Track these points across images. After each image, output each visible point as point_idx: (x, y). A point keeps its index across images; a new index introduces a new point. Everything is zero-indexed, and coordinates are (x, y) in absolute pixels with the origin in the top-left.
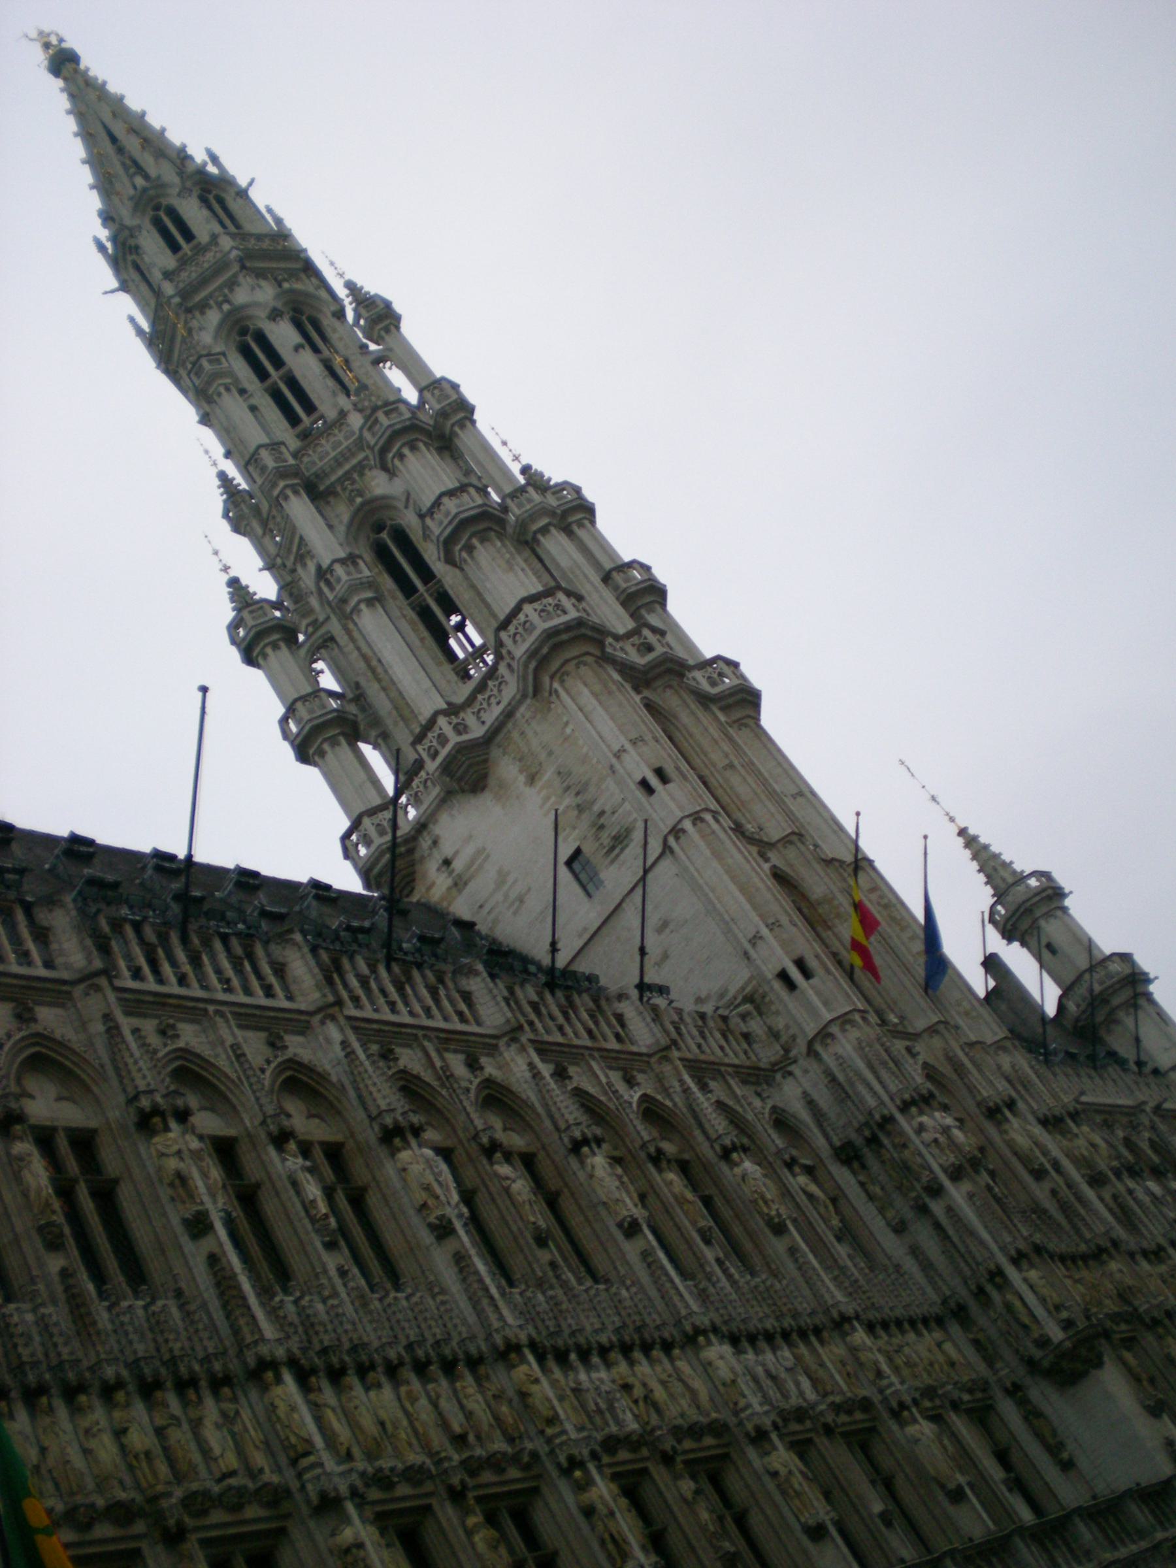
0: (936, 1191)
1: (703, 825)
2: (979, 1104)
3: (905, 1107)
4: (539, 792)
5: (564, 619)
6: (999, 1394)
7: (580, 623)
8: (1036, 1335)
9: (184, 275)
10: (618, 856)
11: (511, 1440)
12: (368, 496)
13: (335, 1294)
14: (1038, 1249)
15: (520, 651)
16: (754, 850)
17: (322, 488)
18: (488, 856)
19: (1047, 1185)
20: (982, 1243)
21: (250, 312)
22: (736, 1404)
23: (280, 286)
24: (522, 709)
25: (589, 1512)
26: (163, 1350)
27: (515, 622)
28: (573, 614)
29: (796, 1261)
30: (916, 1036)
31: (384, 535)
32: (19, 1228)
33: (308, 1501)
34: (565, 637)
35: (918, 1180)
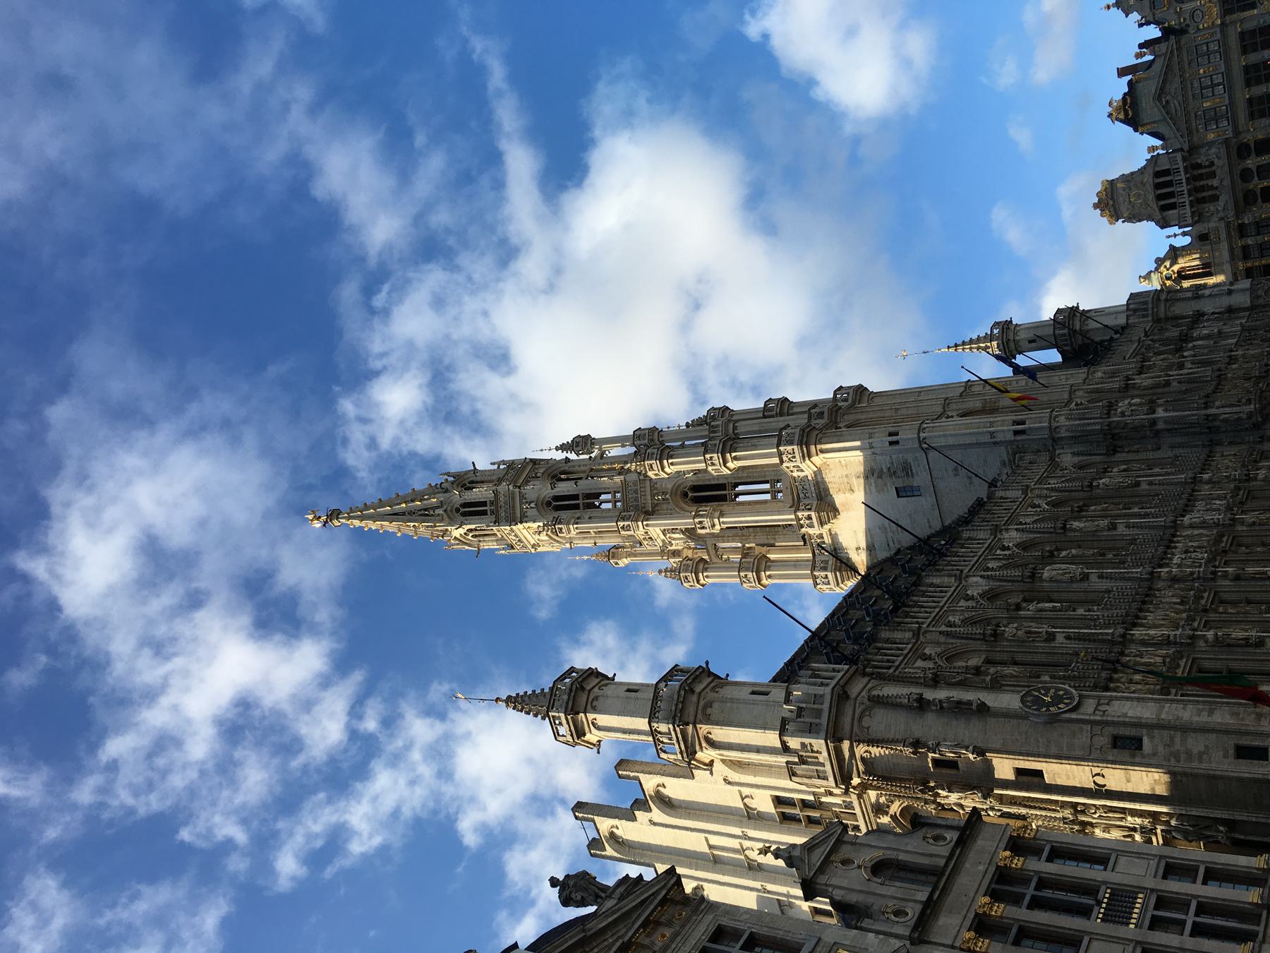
0: (1154, 422)
1: (927, 429)
2: (1119, 392)
6: (1259, 446)
7: (803, 430)
8: (1245, 416)
11: (1191, 590)
13: (1097, 615)
14: (1207, 396)
16: (944, 419)
19: (1175, 384)
20: (1189, 416)
22: (1214, 523)
25: (1237, 578)
29: (1156, 484)
30: (1070, 401)
31: (690, 495)
33: (1189, 644)
35: (1144, 426)
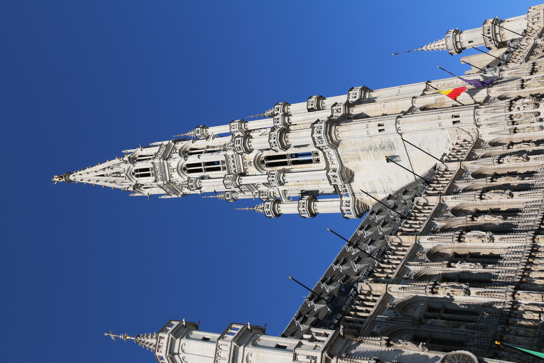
3: (510, 110)
4: (364, 159)
5: (323, 128)
9: (159, 177)
10: (394, 148)
12: (252, 161)
15: (325, 143)
17: (243, 171)
18: (372, 181)
21: (180, 165)
23: (177, 153)
24: (339, 151)
26: (497, 315)
27: (316, 141)
28: (323, 125)
31: (266, 162)
32: (450, 332)
34: (328, 130)
